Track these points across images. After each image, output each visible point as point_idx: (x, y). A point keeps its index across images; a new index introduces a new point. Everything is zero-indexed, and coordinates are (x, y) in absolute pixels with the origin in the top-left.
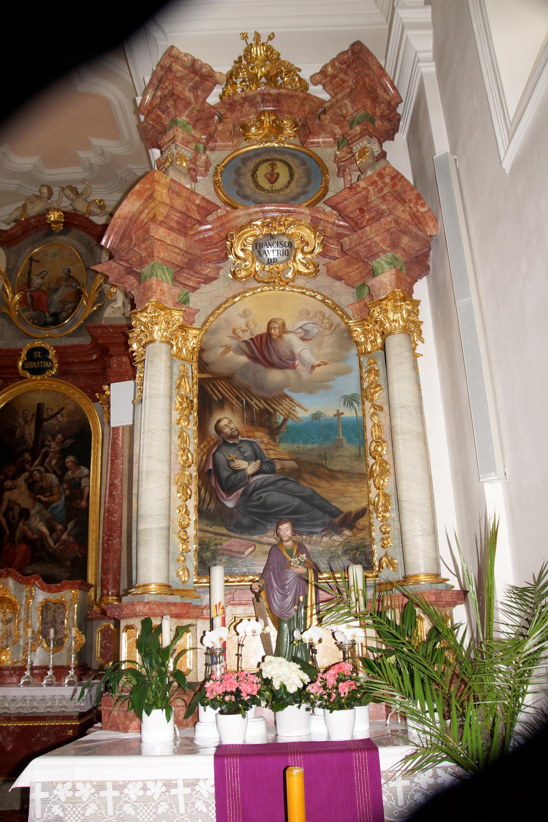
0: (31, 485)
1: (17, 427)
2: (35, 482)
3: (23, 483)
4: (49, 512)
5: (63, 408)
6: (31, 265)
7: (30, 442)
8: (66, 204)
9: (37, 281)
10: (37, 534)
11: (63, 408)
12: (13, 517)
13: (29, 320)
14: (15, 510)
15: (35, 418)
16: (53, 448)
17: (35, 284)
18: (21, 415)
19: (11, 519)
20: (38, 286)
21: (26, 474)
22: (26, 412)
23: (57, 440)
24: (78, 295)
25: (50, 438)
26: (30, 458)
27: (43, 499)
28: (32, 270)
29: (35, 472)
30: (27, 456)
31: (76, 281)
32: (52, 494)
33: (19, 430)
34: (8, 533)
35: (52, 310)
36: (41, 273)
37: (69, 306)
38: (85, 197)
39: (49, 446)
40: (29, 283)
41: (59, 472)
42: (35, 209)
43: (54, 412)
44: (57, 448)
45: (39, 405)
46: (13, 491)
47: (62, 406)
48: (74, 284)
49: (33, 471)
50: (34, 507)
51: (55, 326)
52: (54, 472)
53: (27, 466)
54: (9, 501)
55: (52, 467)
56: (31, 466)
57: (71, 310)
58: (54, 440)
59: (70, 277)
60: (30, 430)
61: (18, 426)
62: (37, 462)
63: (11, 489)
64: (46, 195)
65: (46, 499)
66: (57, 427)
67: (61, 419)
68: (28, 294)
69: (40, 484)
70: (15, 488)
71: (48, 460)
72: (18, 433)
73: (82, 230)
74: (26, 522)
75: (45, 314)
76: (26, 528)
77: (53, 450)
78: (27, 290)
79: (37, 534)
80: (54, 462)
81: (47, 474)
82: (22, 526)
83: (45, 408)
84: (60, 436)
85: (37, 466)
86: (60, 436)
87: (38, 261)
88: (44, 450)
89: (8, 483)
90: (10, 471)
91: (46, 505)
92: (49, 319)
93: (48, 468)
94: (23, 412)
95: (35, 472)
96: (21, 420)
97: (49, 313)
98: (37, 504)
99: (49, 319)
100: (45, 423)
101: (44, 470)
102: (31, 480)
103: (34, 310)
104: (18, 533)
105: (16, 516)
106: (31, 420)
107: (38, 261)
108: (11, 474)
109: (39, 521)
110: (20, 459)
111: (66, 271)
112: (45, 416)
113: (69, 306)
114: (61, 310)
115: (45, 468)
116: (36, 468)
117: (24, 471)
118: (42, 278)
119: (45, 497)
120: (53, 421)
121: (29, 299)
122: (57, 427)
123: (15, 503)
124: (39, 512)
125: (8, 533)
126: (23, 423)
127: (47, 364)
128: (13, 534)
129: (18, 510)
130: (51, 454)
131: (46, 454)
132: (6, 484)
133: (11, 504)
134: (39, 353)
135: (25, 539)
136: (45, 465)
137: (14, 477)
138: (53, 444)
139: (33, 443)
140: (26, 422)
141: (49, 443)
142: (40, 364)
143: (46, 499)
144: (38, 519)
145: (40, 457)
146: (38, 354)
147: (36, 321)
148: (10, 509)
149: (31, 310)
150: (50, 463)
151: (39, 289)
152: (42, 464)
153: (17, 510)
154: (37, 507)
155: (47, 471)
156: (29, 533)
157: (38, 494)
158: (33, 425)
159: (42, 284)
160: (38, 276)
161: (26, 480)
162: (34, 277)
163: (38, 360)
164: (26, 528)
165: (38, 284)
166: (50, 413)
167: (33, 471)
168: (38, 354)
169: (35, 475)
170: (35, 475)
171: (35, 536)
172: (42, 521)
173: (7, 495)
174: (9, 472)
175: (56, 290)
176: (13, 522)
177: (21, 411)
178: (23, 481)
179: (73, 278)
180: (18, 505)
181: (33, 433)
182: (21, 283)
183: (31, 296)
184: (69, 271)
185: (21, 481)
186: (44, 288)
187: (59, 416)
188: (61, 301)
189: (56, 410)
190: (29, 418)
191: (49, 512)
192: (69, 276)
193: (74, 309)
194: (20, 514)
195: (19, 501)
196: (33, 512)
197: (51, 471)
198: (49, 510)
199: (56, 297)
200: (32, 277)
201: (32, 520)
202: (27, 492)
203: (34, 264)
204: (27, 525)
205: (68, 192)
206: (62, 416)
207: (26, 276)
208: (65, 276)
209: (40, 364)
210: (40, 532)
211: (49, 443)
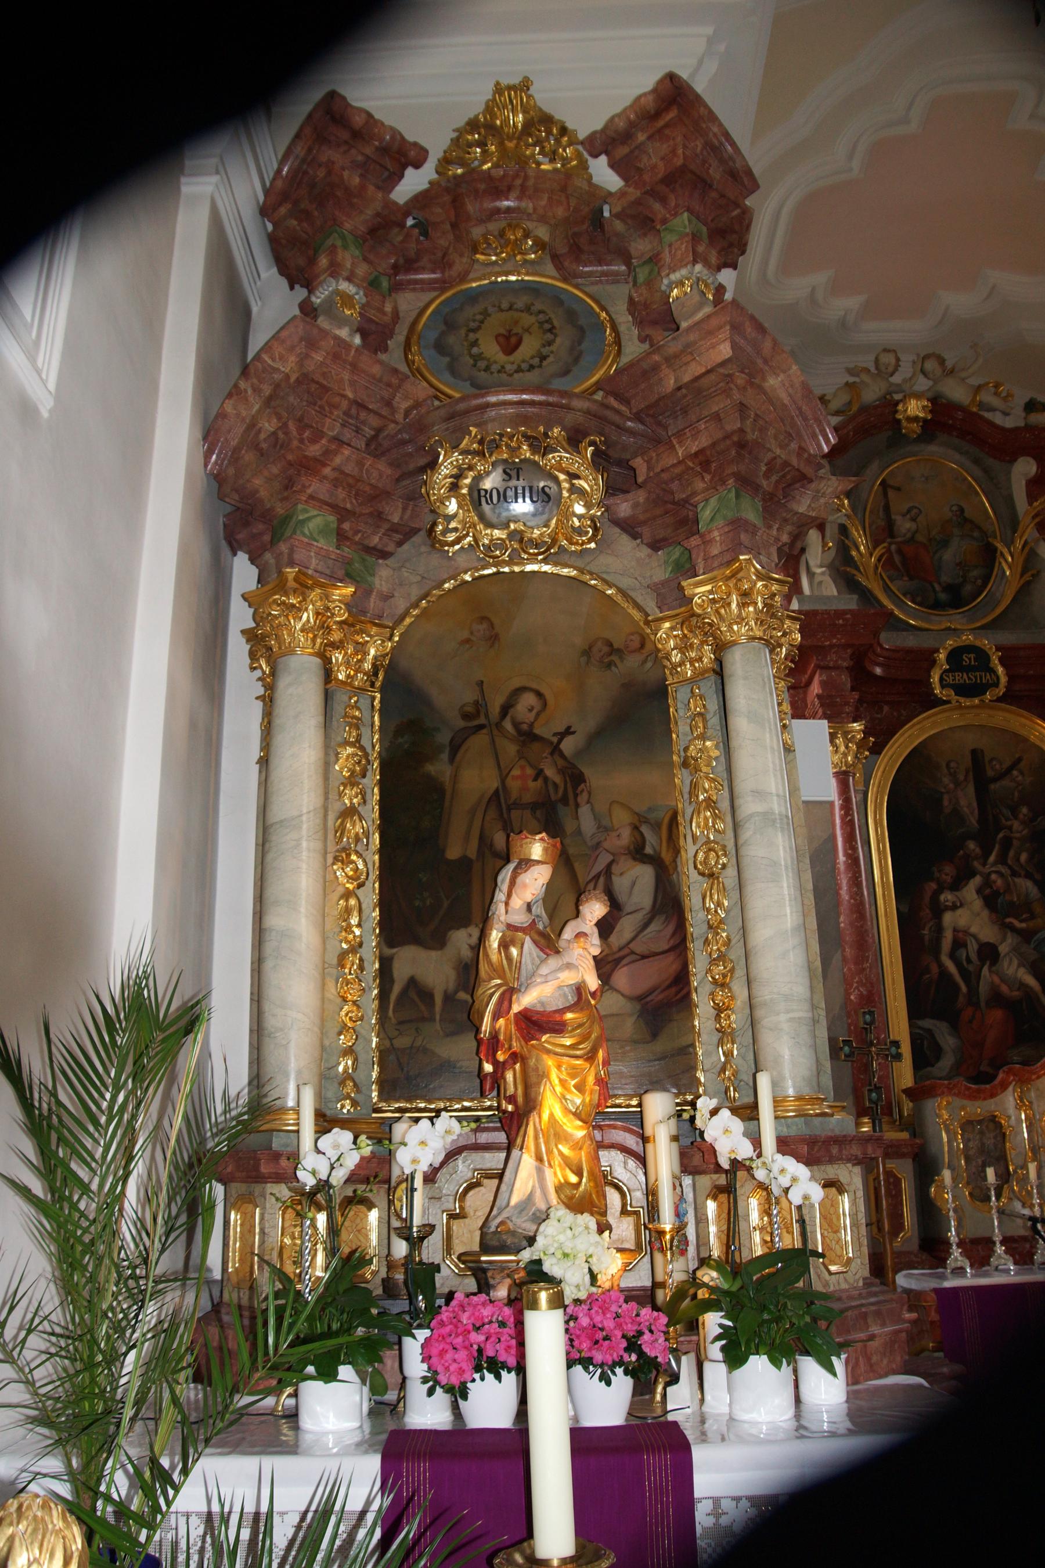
0: (991, 899)
1: (942, 793)
2: (996, 894)
3: (975, 896)
4: (1034, 949)
5: (1020, 760)
6: (885, 495)
7: (973, 820)
8: (922, 384)
9: (904, 526)
10: (1019, 989)
11: (1020, 760)
12: (969, 960)
13: (904, 595)
14: (969, 947)
15: (971, 773)
16: (1018, 832)
17: (904, 531)
18: (945, 771)
19: (965, 963)
20: (909, 535)
21: (977, 880)
22: (952, 765)
23: (1021, 816)
24: (990, 554)
25: (1007, 812)
26: (978, 850)
27: (1017, 924)
28: (891, 504)
29: (993, 876)
30: (971, 845)
31: (978, 528)
32: (1033, 917)
33: (946, 797)
34: (964, 988)
35: (945, 578)
36: (909, 511)
37: (975, 573)
38: (964, 374)
39: (1010, 828)
40: (890, 529)
41: (1038, 876)
42: (872, 393)
43: (1005, 766)
44: (1025, 832)
45: (974, 752)
46: (959, 912)
47: (1017, 756)
48: (976, 534)
49: (989, 874)
50: (1004, 939)
51: (957, 608)
52: (1028, 876)
53: (976, 864)
54: (955, 930)
55: (1022, 866)
56: (984, 865)
57: (979, 582)
58: (1016, 817)
59: (966, 520)
60: (967, 800)
61: (943, 790)
62: (992, 858)
63: (954, 908)
64: (891, 369)
65: (1024, 925)
66: (1016, 794)
67: (1020, 778)
68: (893, 547)
69: (1008, 897)
70: (962, 905)
71: (1011, 853)
72: (946, 803)
73: (957, 437)
74: (994, 969)
75: (933, 587)
76: (996, 980)
77: (1018, 835)
78: (889, 540)
79: (1019, 989)
80: (1024, 857)
81: (1017, 880)
82: (987, 973)
83: (987, 759)
84: (1024, 810)
85: (995, 863)
86: (1024, 810)
87: (899, 489)
88: (1001, 835)
89: (947, 897)
90: (947, 875)
91: (1026, 936)
92: (943, 596)
93: (1016, 868)
94: (948, 765)
95: (993, 876)
96: (946, 780)
97: (940, 583)
98: (1009, 934)
99: (943, 596)
100: (992, 786)
101: (1009, 872)
102: (988, 891)
103: (911, 578)
104: (983, 988)
105: (974, 956)
106: (966, 779)
107: (899, 489)
108: (949, 879)
109: (1019, 966)
110: (961, 852)
111: (954, 508)
112: (990, 773)
113: (975, 573)
114: (961, 579)
115: (1010, 867)
116: (993, 869)
117: (973, 874)
118: (914, 520)
119: (1021, 921)
120: (1006, 783)
121: (897, 558)
122: (1016, 794)
123: (966, 932)
124: (1015, 949)
125: (964, 988)
126: (952, 786)
127: (988, 677)
128: (973, 991)
129: (976, 947)
130: (1015, 842)
131: (1007, 844)
132: (942, 897)
133: (960, 935)
134: (972, 656)
135: (997, 999)
136: (1009, 862)
137: (956, 885)
138: (1016, 825)
139: (978, 822)
140: (957, 784)
141: (1009, 823)
142: (976, 677)
143: (1024, 925)
144: (1015, 962)
145: (997, 847)
146: (970, 659)
147: (919, 599)
148: (958, 944)
149: (906, 578)
150: (1018, 860)
151: (913, 538)
152: (1002, 859)
153: (973, 947)
154: (1009, 940)
155: (1014, 874)
156: (1004, 989)
157: (1008, 916)
158: (971, 789)
159: (916, 531)
160: (904, 515)
161: (979, 891)
162: (898, 519)
163: (969, 669)
164: (996, 980)
165: (909, 530)
166: (998, 767)
167: (989, 874)
168: (970, 659)
169: (995, 882)
170: (995, 882)
171: (1016, 993)
172: (1024, 966)
173: (948, 918)
174: (944, 876)
175: (945, 543)
176: (971, 968)
177: (944, 765)
178: (974, 893)
179: (971, 522)
180: (974, 936)
181: (975, 804)
182: (874, 527)
183: (900, 551)
184: (962, 510)
185: (970, 891)
186: (919, 538)
187: (1015, 773)
188: (959, 564)
189: (1007, 764)
190: (961, 777)
191: (1034, 949)
192: (963, 520)
193: (986, 579)
194: (979, 952)
195: (973, 930)
196: (1003, 949)
197: (1023, 873)
198: (1032, 946)
199: (948, 556)
200: (893, 517)
201: (1006, 964)
202: (986, 913)
203: (891, 494)
204: (997, 974)
205: (929, 365)
206: (1022, 773)
207: (881, 513)
208: (955, 518)
209: (976, 677)
210: (1022, 986)
211: (1009, 823)
